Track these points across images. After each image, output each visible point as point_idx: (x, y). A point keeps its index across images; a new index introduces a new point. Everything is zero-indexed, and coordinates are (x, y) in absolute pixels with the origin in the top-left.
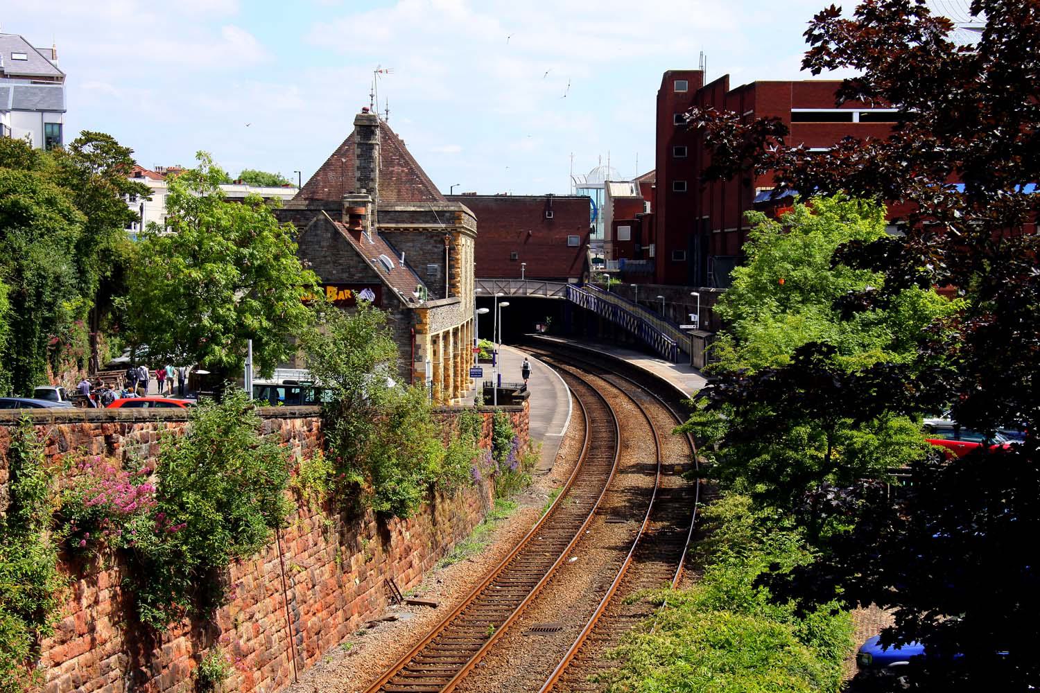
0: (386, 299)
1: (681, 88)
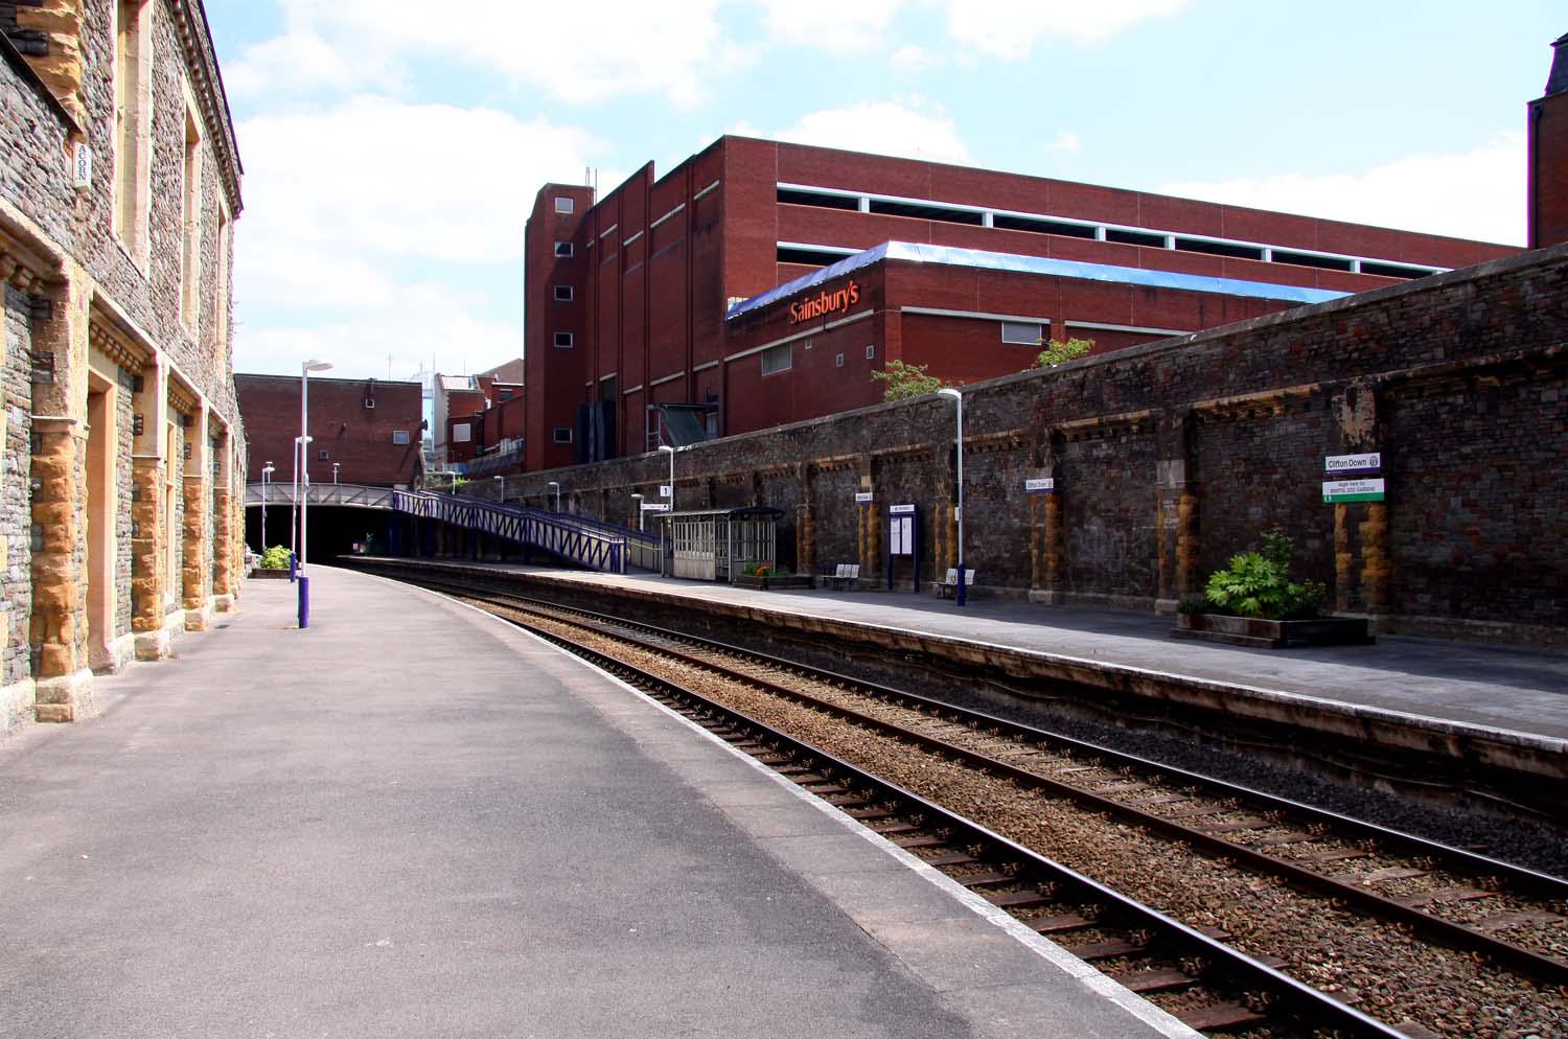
1: (564, 206)
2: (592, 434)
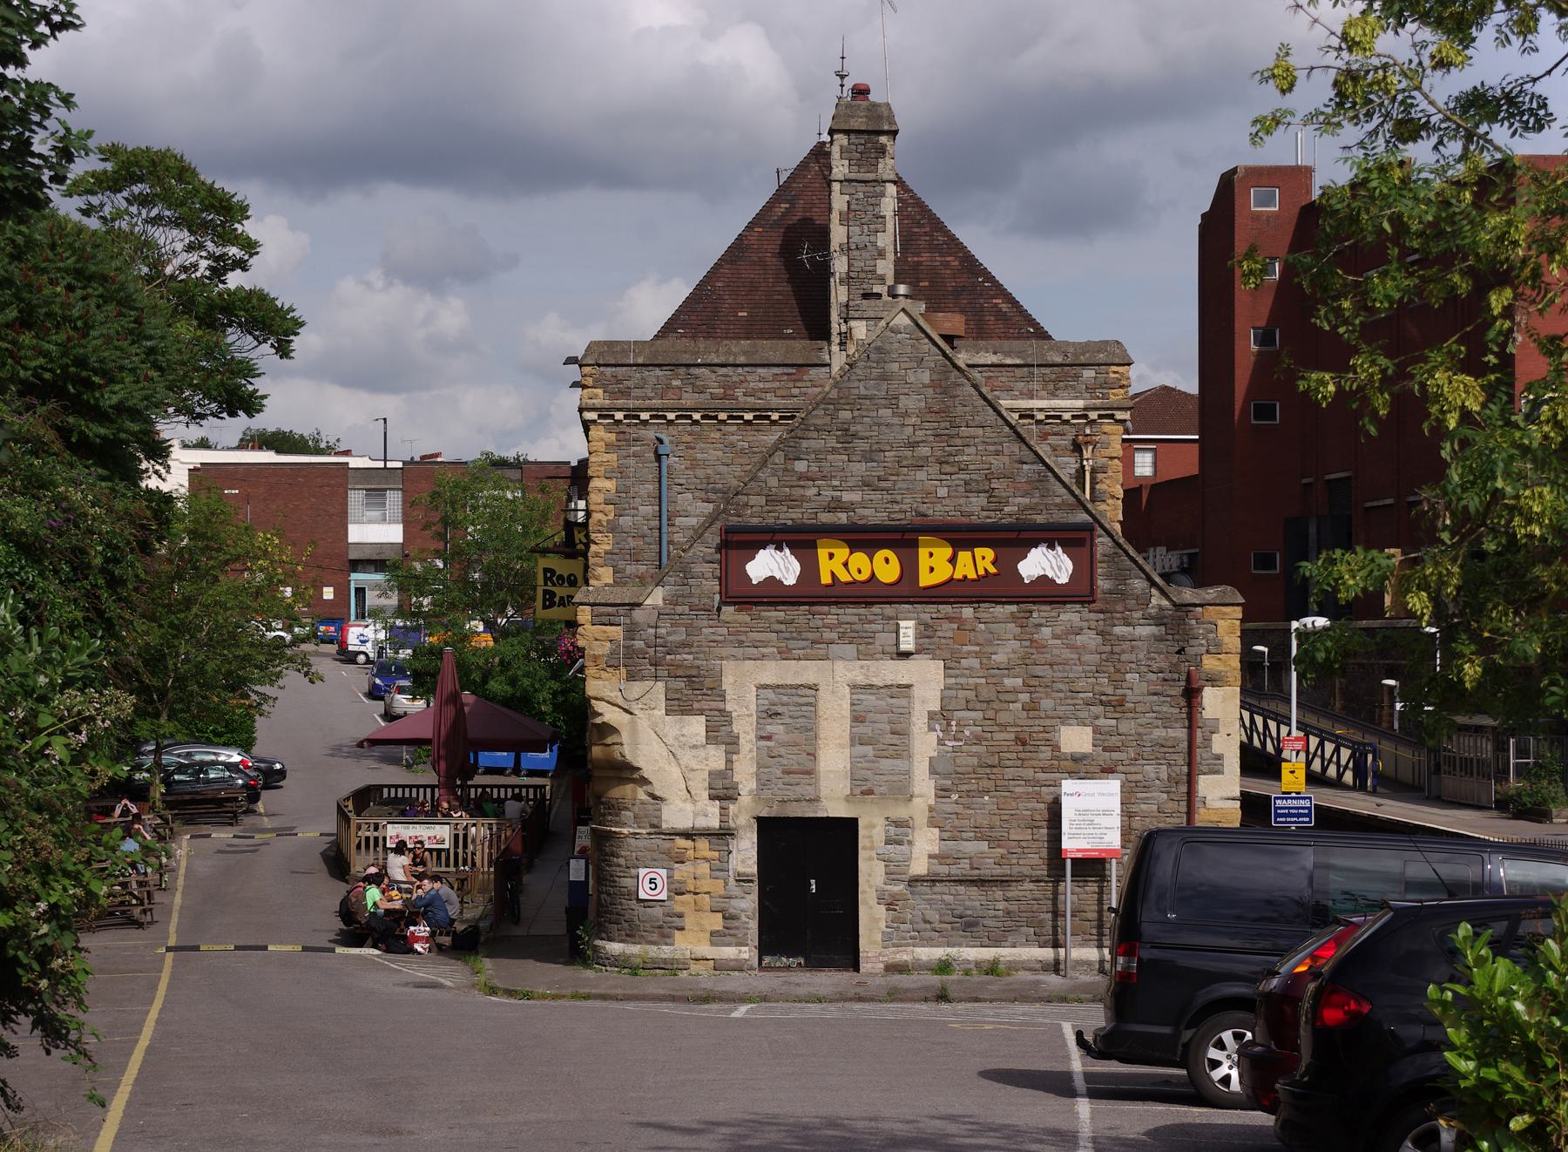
0: (1108, 576)
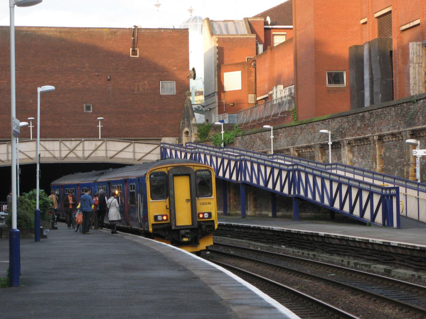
2: (367, 76)
